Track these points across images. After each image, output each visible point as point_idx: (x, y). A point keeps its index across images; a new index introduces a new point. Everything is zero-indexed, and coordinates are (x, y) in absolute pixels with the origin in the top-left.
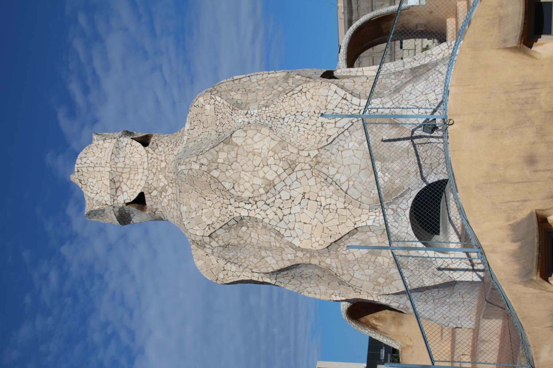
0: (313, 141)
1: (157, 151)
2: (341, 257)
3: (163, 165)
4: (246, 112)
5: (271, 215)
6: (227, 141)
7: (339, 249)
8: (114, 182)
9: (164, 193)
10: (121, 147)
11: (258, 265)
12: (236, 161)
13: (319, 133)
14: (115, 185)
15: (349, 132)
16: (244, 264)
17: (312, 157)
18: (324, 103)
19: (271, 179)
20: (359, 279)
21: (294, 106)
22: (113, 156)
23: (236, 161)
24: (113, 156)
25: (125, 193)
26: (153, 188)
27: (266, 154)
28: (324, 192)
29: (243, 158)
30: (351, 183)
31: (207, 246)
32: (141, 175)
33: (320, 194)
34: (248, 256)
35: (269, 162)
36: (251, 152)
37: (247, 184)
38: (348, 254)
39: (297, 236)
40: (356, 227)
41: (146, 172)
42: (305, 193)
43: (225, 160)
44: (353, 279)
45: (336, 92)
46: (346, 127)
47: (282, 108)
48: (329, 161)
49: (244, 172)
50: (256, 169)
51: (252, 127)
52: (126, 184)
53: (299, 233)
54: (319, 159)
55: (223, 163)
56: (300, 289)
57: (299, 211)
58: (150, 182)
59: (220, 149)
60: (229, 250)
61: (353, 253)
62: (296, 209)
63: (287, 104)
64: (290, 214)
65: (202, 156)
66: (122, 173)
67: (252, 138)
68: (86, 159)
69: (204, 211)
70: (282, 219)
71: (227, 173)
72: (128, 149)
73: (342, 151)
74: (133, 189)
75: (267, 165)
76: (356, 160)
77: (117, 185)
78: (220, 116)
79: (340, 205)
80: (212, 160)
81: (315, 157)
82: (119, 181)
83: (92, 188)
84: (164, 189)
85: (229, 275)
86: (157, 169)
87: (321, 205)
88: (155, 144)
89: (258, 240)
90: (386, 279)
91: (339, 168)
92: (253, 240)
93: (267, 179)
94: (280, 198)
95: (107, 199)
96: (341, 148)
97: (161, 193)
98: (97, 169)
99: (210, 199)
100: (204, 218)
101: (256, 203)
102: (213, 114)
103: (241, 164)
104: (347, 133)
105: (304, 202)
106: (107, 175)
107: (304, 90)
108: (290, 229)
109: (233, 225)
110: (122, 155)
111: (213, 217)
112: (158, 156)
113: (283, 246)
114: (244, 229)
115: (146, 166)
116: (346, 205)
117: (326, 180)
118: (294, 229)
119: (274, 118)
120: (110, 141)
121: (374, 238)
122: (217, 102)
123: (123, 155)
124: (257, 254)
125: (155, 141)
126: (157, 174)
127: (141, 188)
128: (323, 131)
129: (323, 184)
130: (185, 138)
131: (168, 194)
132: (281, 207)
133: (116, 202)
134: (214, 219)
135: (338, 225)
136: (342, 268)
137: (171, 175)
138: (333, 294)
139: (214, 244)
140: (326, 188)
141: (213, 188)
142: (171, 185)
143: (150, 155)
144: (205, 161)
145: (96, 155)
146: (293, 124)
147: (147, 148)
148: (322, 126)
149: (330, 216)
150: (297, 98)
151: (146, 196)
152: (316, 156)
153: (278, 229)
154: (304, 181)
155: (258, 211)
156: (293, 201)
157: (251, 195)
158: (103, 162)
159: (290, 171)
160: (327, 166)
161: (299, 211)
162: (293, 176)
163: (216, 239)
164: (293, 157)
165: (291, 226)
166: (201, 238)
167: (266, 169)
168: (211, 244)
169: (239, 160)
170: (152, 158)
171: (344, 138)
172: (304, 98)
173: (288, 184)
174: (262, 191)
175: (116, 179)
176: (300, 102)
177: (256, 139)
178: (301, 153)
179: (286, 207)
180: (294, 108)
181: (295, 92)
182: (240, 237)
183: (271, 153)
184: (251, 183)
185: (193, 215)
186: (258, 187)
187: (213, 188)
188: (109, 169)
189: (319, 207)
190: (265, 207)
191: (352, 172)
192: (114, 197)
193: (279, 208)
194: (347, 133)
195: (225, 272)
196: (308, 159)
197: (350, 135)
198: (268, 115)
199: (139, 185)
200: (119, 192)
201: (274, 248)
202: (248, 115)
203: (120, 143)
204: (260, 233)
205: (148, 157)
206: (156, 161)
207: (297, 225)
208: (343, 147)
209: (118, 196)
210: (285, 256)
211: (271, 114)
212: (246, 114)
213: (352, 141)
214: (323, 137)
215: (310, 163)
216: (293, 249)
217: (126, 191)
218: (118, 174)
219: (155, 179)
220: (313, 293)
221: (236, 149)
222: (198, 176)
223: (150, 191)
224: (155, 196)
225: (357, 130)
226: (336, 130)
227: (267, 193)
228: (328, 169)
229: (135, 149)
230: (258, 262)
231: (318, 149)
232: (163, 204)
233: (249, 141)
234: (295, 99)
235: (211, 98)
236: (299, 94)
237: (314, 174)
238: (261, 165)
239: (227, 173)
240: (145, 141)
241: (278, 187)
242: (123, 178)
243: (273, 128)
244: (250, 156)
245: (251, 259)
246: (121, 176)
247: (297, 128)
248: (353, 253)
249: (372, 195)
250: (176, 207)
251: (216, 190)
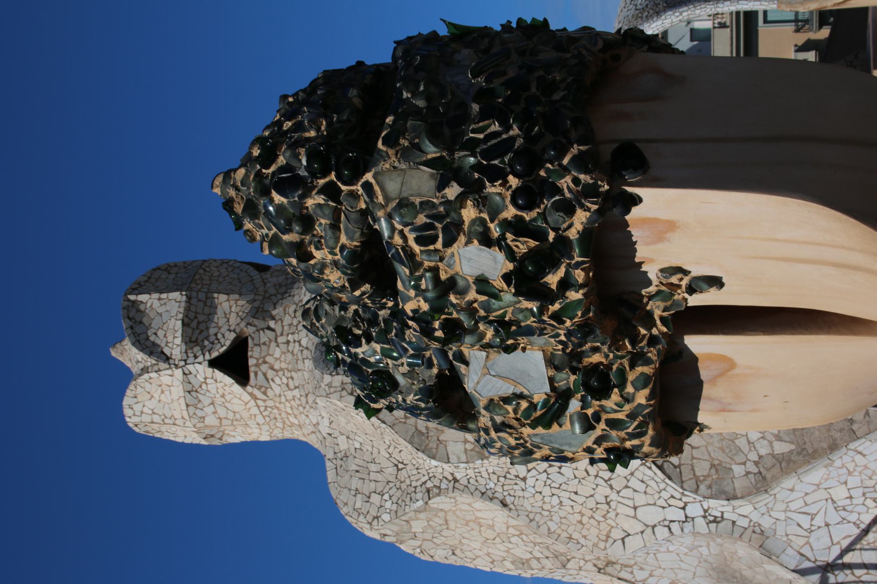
0: (594, 532)
1: (270, 393)
10: (197, 386)
13: (604, 516)
68: (141, 405)
72: (212, 387)
86: (284, 423)
110: (206, 401)
112: (277, 405)
119: (505, 477)
120: (169, 372)
123: (209, 401)
125: (257, 365)
128: (612, 515)
145: (156, 396)
146: (547, 491)
147: (248, 388)
160: (630, 570)
170: (266, 407)
198: (491, 471)
205: (258, 407)
206: (275, 411)
211: (496, 469)
214: (612, 527)
215: (595, 562)
239: (434, 540)
243: (509, 500)
247: (555, 500)
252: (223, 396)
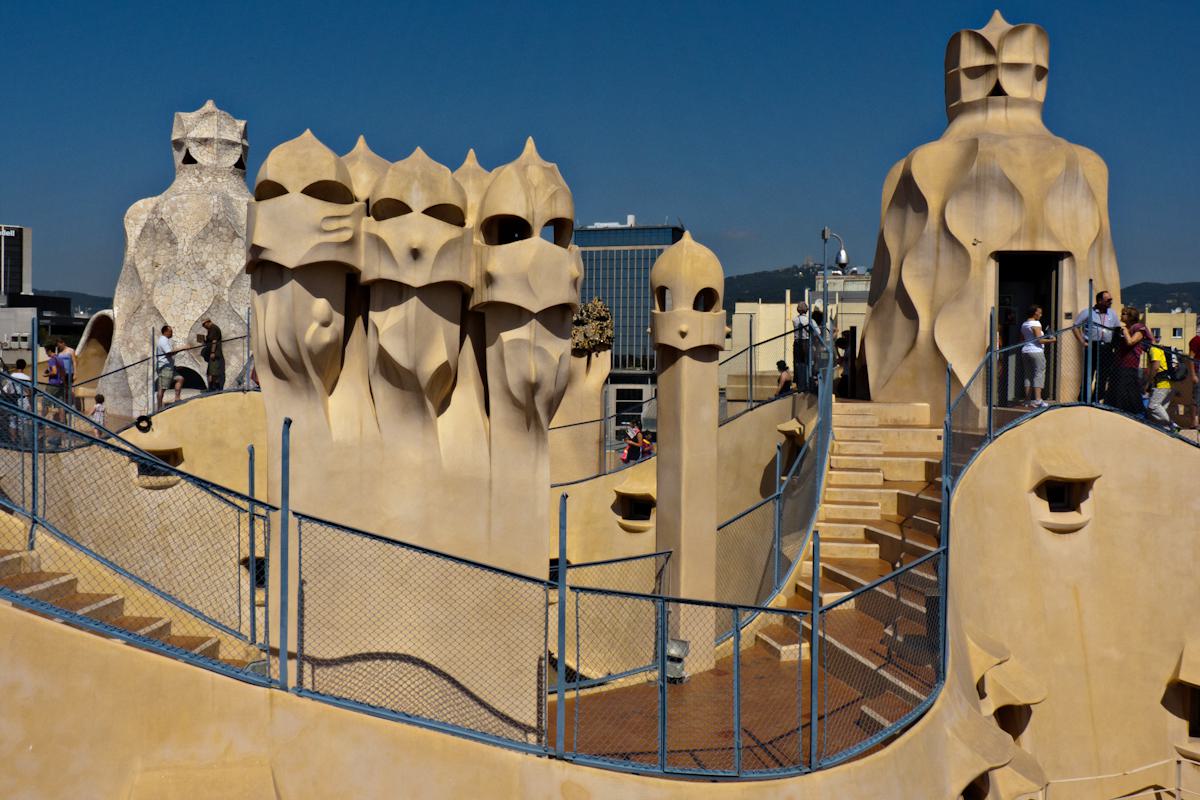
2: (148, 317)
3: (219, 180)
5: (179, 266)
14: (204, 142)
53: (166, 286)
79: (187, 317)
84: (200, 180)
92: (159, 252)
95: (192, 134)
97: (197, 177)
114: (169, 245)
130: (240, 199)
134: (175, 222)
137: (211, 187)
139: (156, 221)
144: (220, 217)
159: (213, 280)
162: (208, 283)
167: (214, 263)
174: (197, 260)
192: (194, 140)
210: (147, 274)
231: (229, 302)
240: (240, 165)
241: (200, 272)
244: (224, 251)
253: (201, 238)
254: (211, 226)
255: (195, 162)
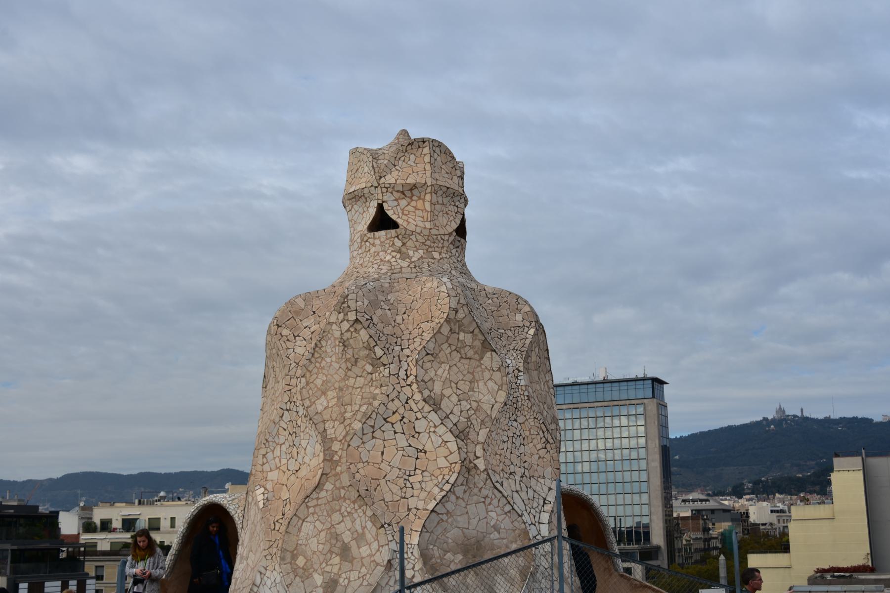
3: (436, 255)
4: (521, 369)
5: (392, 406)
6: (486, 346)
7: (348, 501)
8: (411, 190)
9: (398, 256)
11: (312, 385)
12: (462, 357)
14: (410, 191)
15: (509, 512)
16: (313, 365)
17: (475, 462)
18: (536, 475)
19: (442, 406)
20: (300, 530)
21: (530, 434)
22: (444, 189)
23: (462, 357)
24: (444, 189)
25: (396, 203)
26: (405, 241)
27: (473, 398)
28: (429, 479)
29: (466, 366)
30: (445, 517)
31: (341, 316)
32: (422, 225)
33: (425, 474)
34: (326, 372)
35: (464, 403)
36: (474, 378)
37: (433, 372)
38: (342, 514)
39: (363, 443)
40: (386, 526)
41: (426, 232)
42: (425, 452)
43: (463, 342)
44: (301, 521)
45: (550, 489)
46: (515, 507)
47: (528, 417)
48: (471, 486)
49: (447, 368)
50: (453, 385)
51: (505, 378)
52: (409, 204)
53: (369, 446)
54: (473, 472)
55: (458, 339)
56: (271, 443)
57: (399, 445)
58: (413, 237)
59: (476, 335)
60: (335, 347)
61: (343, 521)
62: (402, 441)
63: (532, 424)
64: (395, 433)
65: (467, 312)
66: (424, 200)
67: (490, 379)
69: (388, 312)
70: (387, 422)
71: (446, 345)
72: (452, 208)
73: (484, 502)
74: (403, 214)
75: (459, 401)
76: (474, 522)
77: (408, 194)
78: (510, 333)
80: (463, 325)
81: (475, 465)
82: (413, 195)
83: (402, 159)
84: (404, 256)
85: (288, 343)
86: (430, 247)
87: (410, 476)
88: (458, 244)
89: (353, 387)
90: (303, 568)
91: (463, 499)
92: (352, 381)
93: (442, 400)
94: (417, 419)
96: (488, 501)
97: (399, 251)
98: (428, 167)
99: (406, 321)
100: (379, 312)
101: (410, 385)
102: (511, 324)
103: (459, 365)
104: (508, 508)
105: (412, 452)
106: (420, 180)
107: (548, 446)
108: (373, 432)
109: (374, 352)
110: (446, 200)
111: (383, 325)
113: (347, 422)
114: (369, 368)
115: (434, 232)
116: (414, 511)
117: (447, 482)
118: (373, 437)
121: (368, 552)
122: (526, 329)
124: (329, 385)
126: (425, 247)
127: (405, 224)
128: (506, 476)
129: (440, 478)
131: (399, 261)
132: (404, 420)
133: (384, 190)
134: (380, 326)
135: (383, 500)
136: (317, 505)
138: (266, 489)
140: (435, 482)
141: (422, 325)
142: (412, 266)
143: (446, 237)
144: (461, 315)
145: (443, 167)
146: (510, 434)
147: (454, 234)
148: (511, 474)
149: (395, 489)
150: (539, 437)
151: (393, 231)
152: (476, 467)
153: (374, 416)
154: (443, 451)
155: (398, 387)
156: (413, 436)
157: (419, 379)
158: (436, 176)
161: (399, 445)
162: (449, 437)
163: (352, 329)
164: (472, 435)
165: (378, 434)
166: (353, 306)
167: (454, 399)
168: (345, 322)
169: (462, 361)
171: (501, 505)
172: (539, 446)
173: (437, 430)
174: (426, 393)
175: (415, 192)
176: (535, 441)
177: (491, 384)
178: (479, 447)
179: (404, 426)
180: (527, 433)
181: (546, 434)
182: (356, 360)
183: (474, 405)
184: (435, 378)
185: (381, 297)
186: (431, 389)
187: (422, 325)
188: (429, 183)
189: (408, 473)
190: (403, 398)
191: (459, 518)
193: (403, 417)
194: (508, 508)
195: (291, 337)
196: (472, 457)
197: (506, 513)
198: (519, 399)
199: (409, 223)
200: (397, 195)
201: (343, 410)
202: (516, 372)
203: (458, 198)
204: (363, 391)
206: (440, 245)
207: (379, 442)
208: (490, 504)
209: (392, 193)
212: (517, 369)
213: (498, 515)
216: (344, 437)
217: (399, 205)
218: (423, 194)
219: (417, 244)
220: (265, 460)
221: (477, 357)
222: (439, 306)
223: (400, 237)
224: (393, 244)
225: (512, 522)
226: (510, 493)
227: (424, 400)
228: (462, 485)
229: (452, 218)
230: (316, 386)
231: (486, 470)
232: (381, 253)
233: (487, 375)
234: (538, 434)
235: (531, 322)
236: (544, 440)
237: (453, 465)
238: (459, 392)
239: (446, 345)
242: (416, 201)
245: (320, 376)
246: (419, 198)
247: (506, 439)
248: (343, 521)
249: (431, 547)
250: (383, 271)
251: (421, 330)
252: (447, 213)
253: (429, 355)
254: (446, 330)
255: (394, 225)
